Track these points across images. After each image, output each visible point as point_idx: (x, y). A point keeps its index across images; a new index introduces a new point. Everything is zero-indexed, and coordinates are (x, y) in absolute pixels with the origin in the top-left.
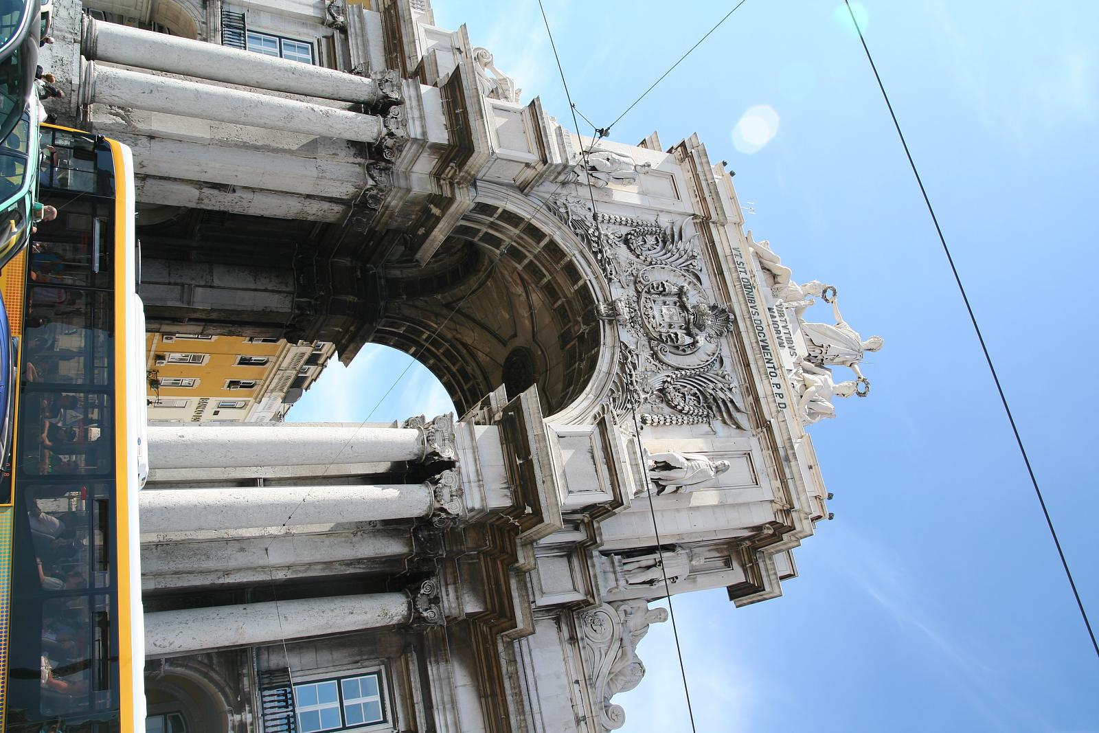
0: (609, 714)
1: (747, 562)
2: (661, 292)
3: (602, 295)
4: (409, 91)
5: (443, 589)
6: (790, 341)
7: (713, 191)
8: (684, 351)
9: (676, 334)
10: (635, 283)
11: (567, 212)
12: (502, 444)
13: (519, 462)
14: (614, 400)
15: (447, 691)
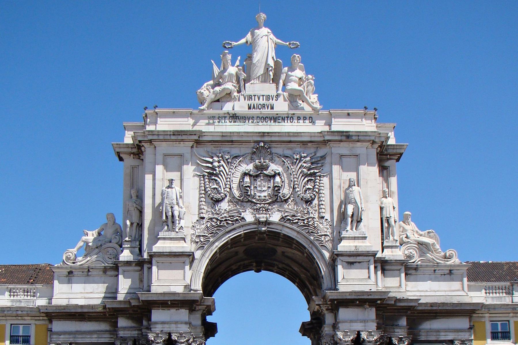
0: (450, 258)
1: (387, 157)
2: (250, 188)
3: (253, 225)
4: (158, 328)
5: (396, 334)
6: (268, 98)
7: (179, 133)
8: (283, 182)
9: (276, 186)
10: (242, 202)
11: (203, 236)
12: (348, 308)
13: (358, 303)
14: (312, 232)
15: (432, 333)
